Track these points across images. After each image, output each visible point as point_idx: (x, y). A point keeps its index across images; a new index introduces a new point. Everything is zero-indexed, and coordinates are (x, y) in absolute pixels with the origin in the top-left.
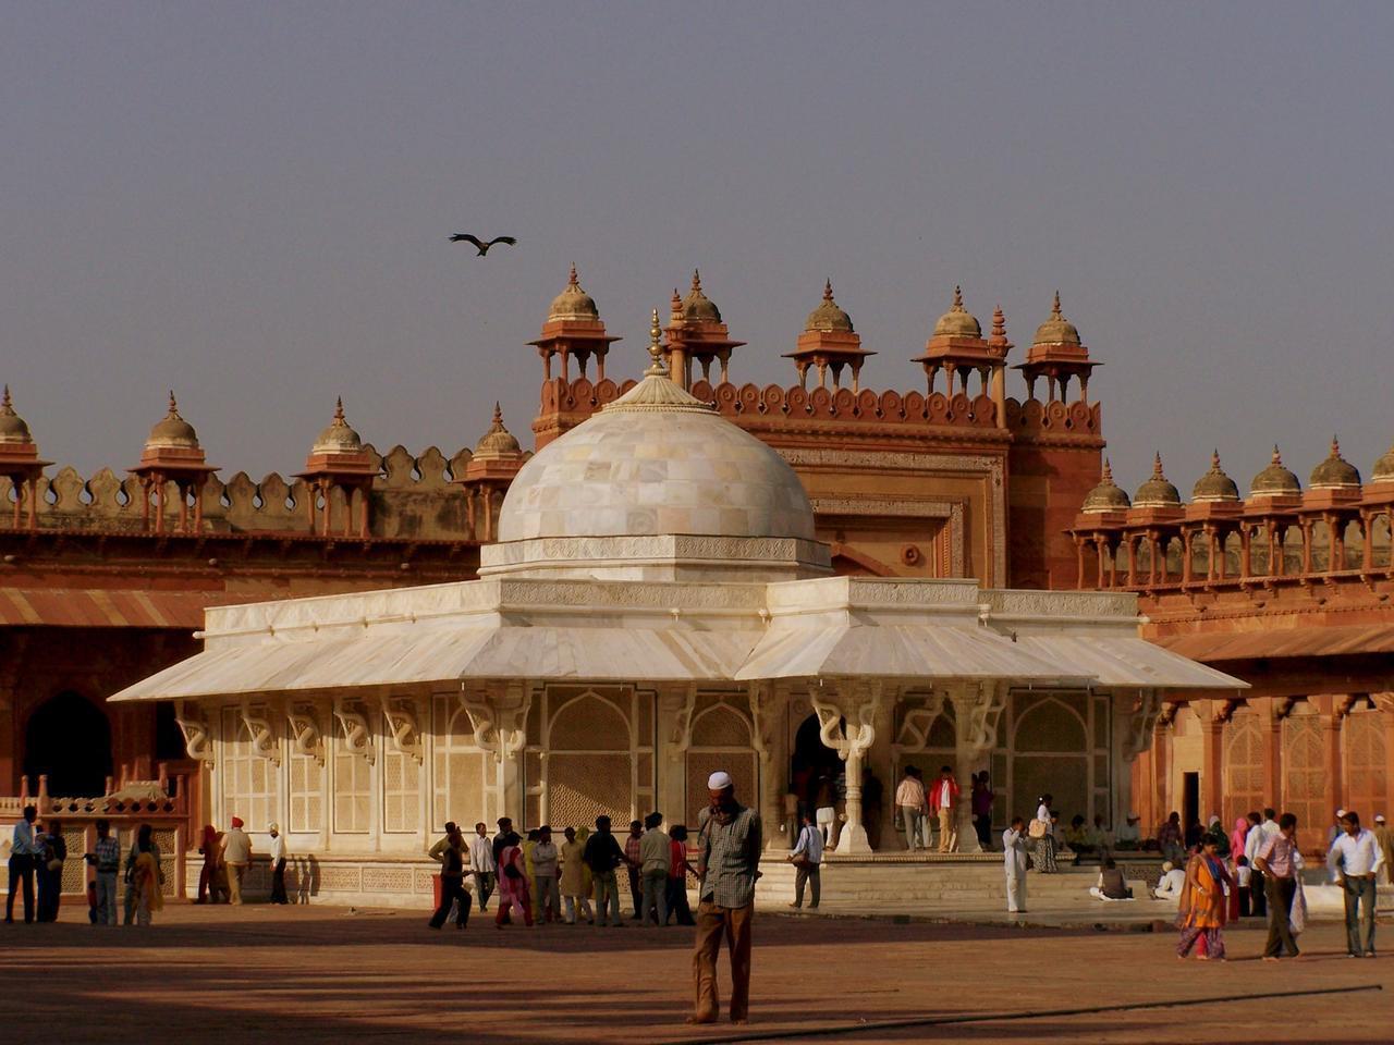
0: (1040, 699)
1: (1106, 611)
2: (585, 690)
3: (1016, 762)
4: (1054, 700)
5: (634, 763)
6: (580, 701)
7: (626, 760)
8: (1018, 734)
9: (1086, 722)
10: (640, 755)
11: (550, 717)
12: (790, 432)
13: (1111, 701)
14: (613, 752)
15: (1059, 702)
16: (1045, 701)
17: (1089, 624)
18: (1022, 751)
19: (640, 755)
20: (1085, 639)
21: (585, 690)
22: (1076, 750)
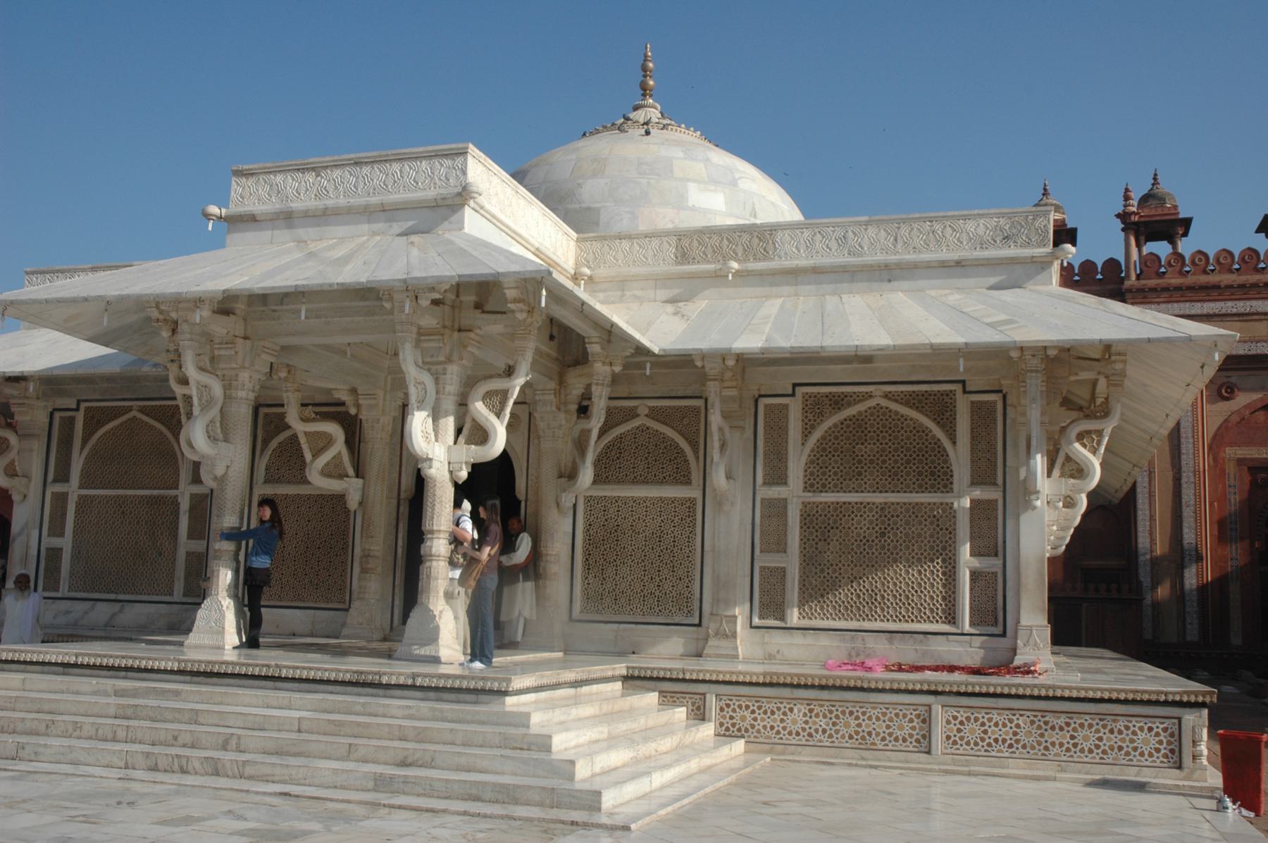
0: (849, 404)
1: (982, 244)
2: (130, 409)
3: (810, 517)
4: (884, 403)
5: (185, 505)
6: (122, 424)
7: (175, 502)
8: (812, 462)
9: (954, 443)
10: (193, 496)
11: (85, 442)
12: (1242, 286)
13: (1004, 397)
14: (155, 492)
15: (894, 406)
16: (861, 407)
17: (943, 265)
18: (824, 489)
19: (193, 496)
20: (933, 293)
21: (130, 409)
22: (933, 489)
